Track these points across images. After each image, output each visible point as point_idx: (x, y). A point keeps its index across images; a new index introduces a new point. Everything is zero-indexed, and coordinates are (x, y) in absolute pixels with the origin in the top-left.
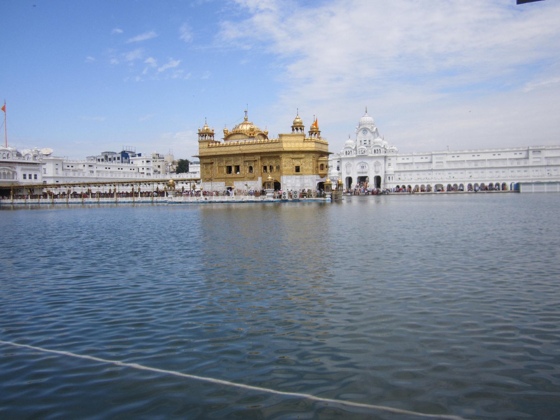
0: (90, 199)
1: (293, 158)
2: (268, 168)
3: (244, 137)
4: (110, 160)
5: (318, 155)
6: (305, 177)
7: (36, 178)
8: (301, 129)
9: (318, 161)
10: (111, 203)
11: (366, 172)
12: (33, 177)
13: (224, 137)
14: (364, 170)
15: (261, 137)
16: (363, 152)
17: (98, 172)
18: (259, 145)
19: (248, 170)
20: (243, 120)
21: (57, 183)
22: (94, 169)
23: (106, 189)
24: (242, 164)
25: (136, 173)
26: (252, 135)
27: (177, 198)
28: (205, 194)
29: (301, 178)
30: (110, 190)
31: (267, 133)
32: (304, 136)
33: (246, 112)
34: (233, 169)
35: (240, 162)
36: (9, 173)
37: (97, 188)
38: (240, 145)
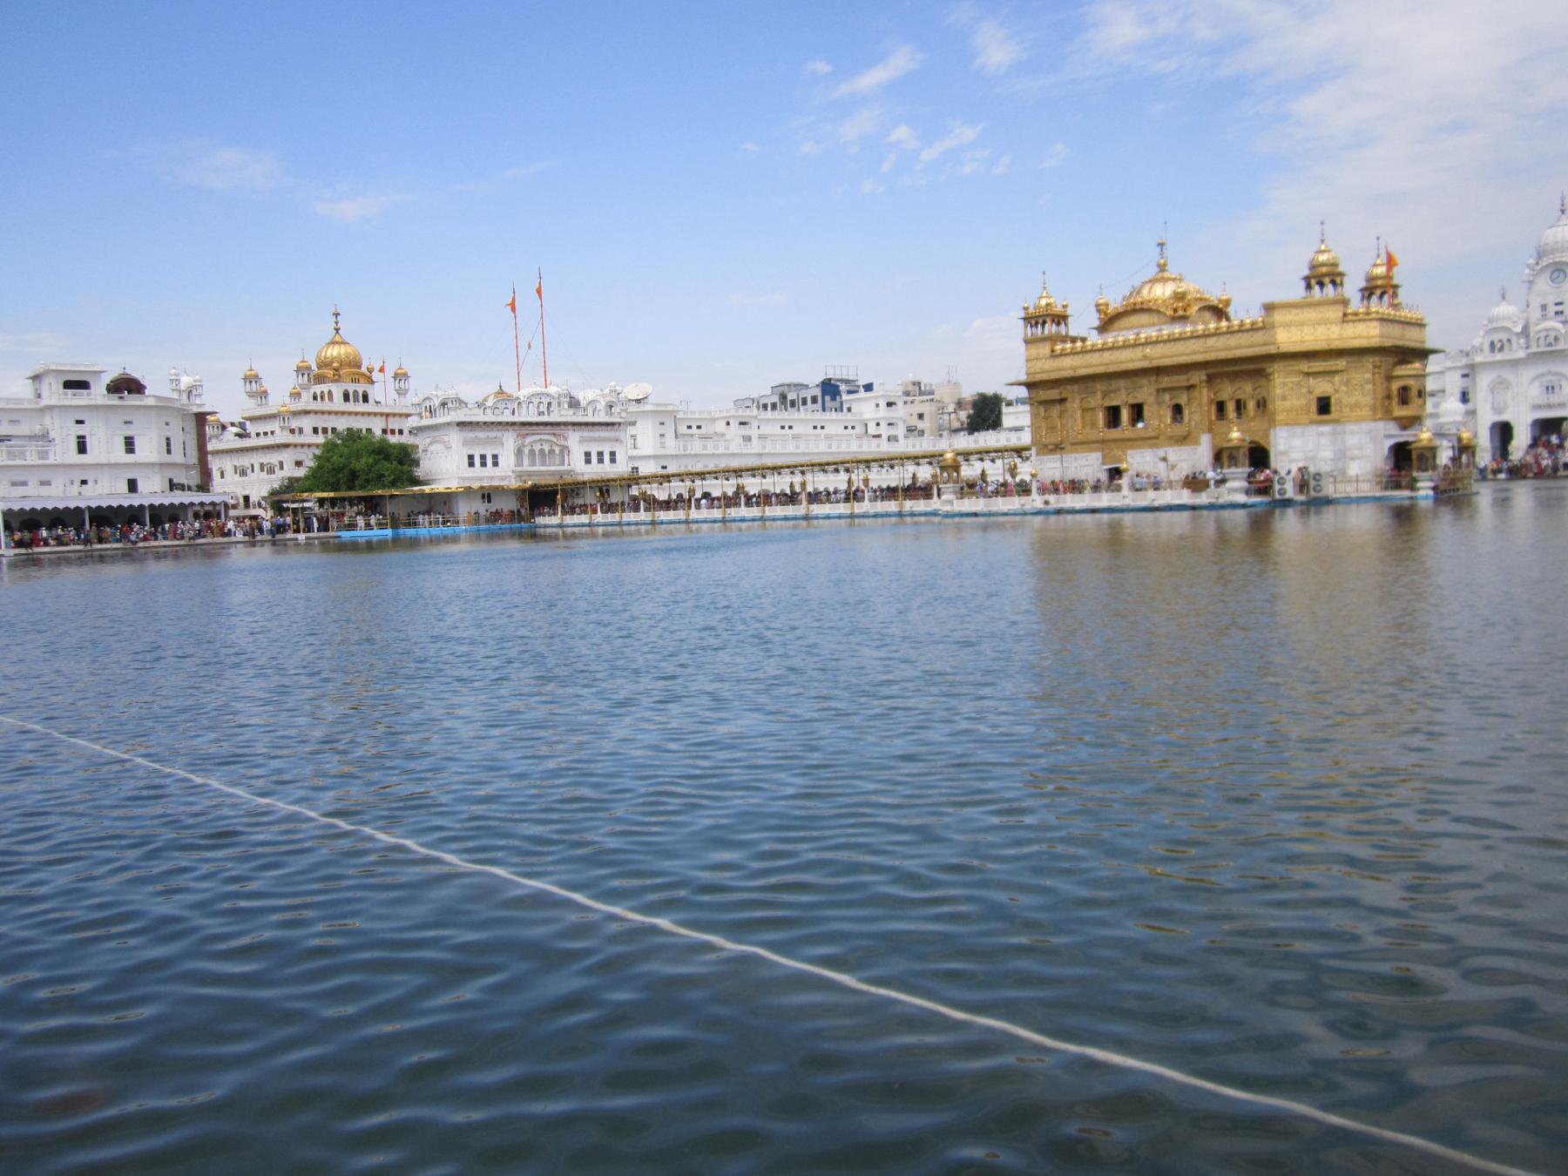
0: (743, 511)
1: (1308, 374)
2: (1230, 408)
3: (1155, 318)
4: (793, 404)
5: (1391, 360)
6: (1350, 427)
7: (613, 460)
8: (1333, 283)
9: (1390, 378)
10: (795, 518)
11: (1561, 405)
12: (607, 457)
13: (1096, 323)
14: (1554, 399)
15: (1207, 315)
16: (1551, 339)
17: (761, 437)
18: (1201, 341)
19: (1168, 416)
20: (1152, 271)
21: (664, 472)
22: (752, 431)
23: (779, 484)
24: (1151, 399)
25: (859, 437)
26: (1181, 313)
27: (966, 500)
28: (1043, 490)
29: (1334, 434)
30: (792, 485)
31: (1228, 303)
32: (1345, 303)
33: (1161, 245)
34: (1125, 415)
35: (1144, 393)
36: (552, 451)
37: (757, 480)
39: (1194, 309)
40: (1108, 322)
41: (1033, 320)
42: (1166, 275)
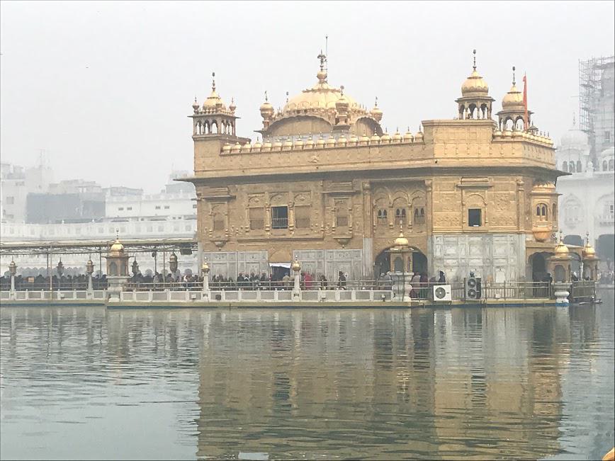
1: (462, 188)
3: (318, 126)
8: (483, 107)
9: (530, 195)
13: (261, 127)
15: (363, 127)
26: (342, 123)
27: (135, 293)
29: (483, 245)
31: (379, 116)
32: (492, 125)
33: (322, 57)
38: (304, 151)
39: (354, 120)
40: (273, 125)
41: (203, 117)
42: (325, 86)
